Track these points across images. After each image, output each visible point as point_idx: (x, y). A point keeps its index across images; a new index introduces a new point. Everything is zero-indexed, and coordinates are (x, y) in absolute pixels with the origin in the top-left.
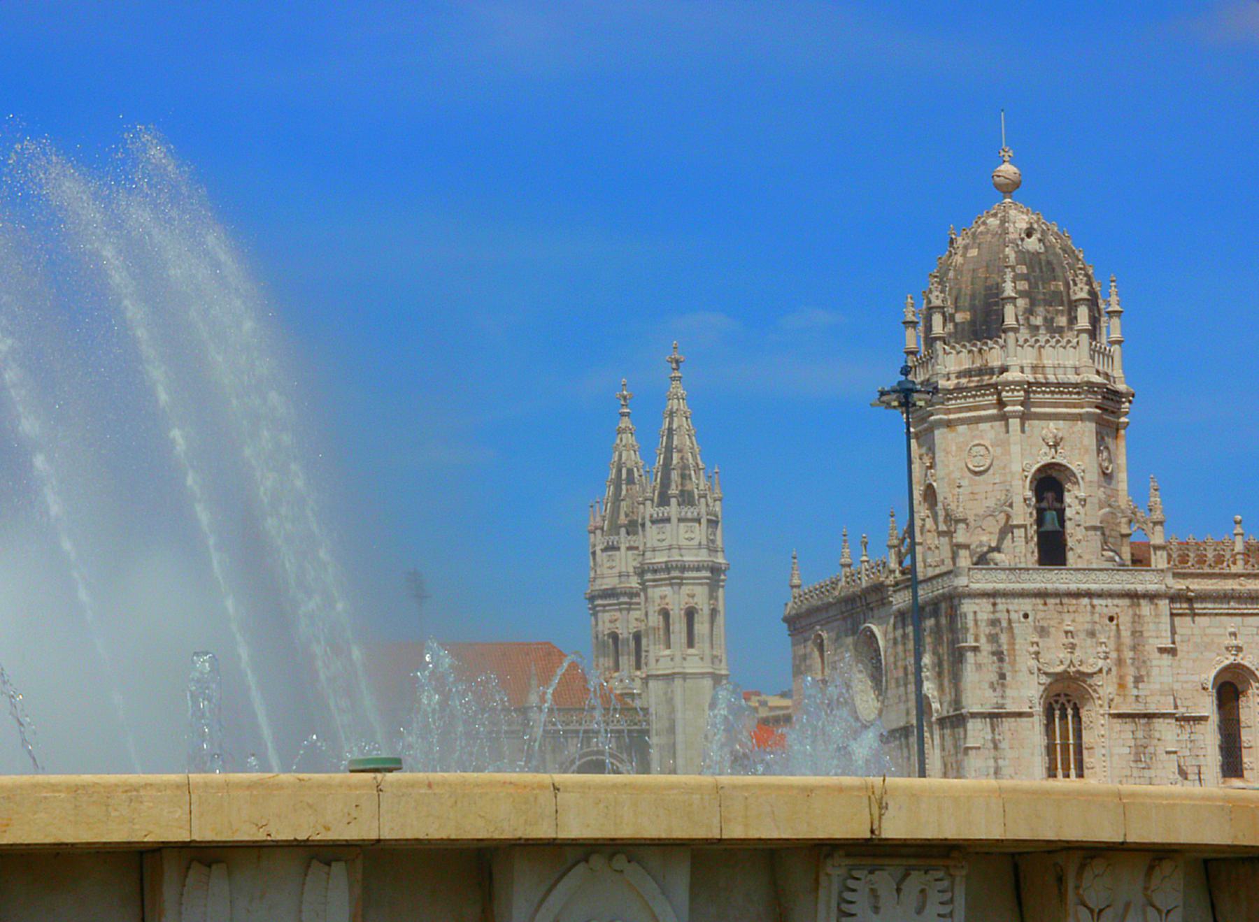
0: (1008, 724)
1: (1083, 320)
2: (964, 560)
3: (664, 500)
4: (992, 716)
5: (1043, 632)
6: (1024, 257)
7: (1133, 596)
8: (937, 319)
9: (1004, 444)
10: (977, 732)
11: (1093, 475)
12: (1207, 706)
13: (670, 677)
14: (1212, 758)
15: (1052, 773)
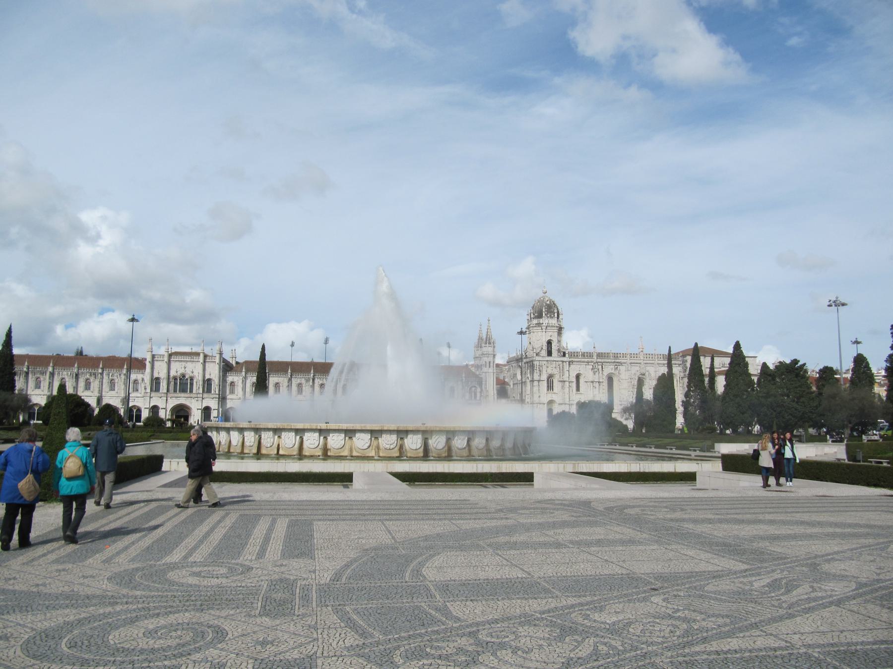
0: (541, 382)
1: (556, 315)
2: (535, 354)
3: (486, 344)
4: (539, 381)
5: (547, 367)
6: (547, 304)
7: (563, 362)
8: (532, 314)
9: (542, 336)
10: (536, 383)
11: (557, 341)
12: (574, 380)
13: (486, 373)
15: (548, 390)
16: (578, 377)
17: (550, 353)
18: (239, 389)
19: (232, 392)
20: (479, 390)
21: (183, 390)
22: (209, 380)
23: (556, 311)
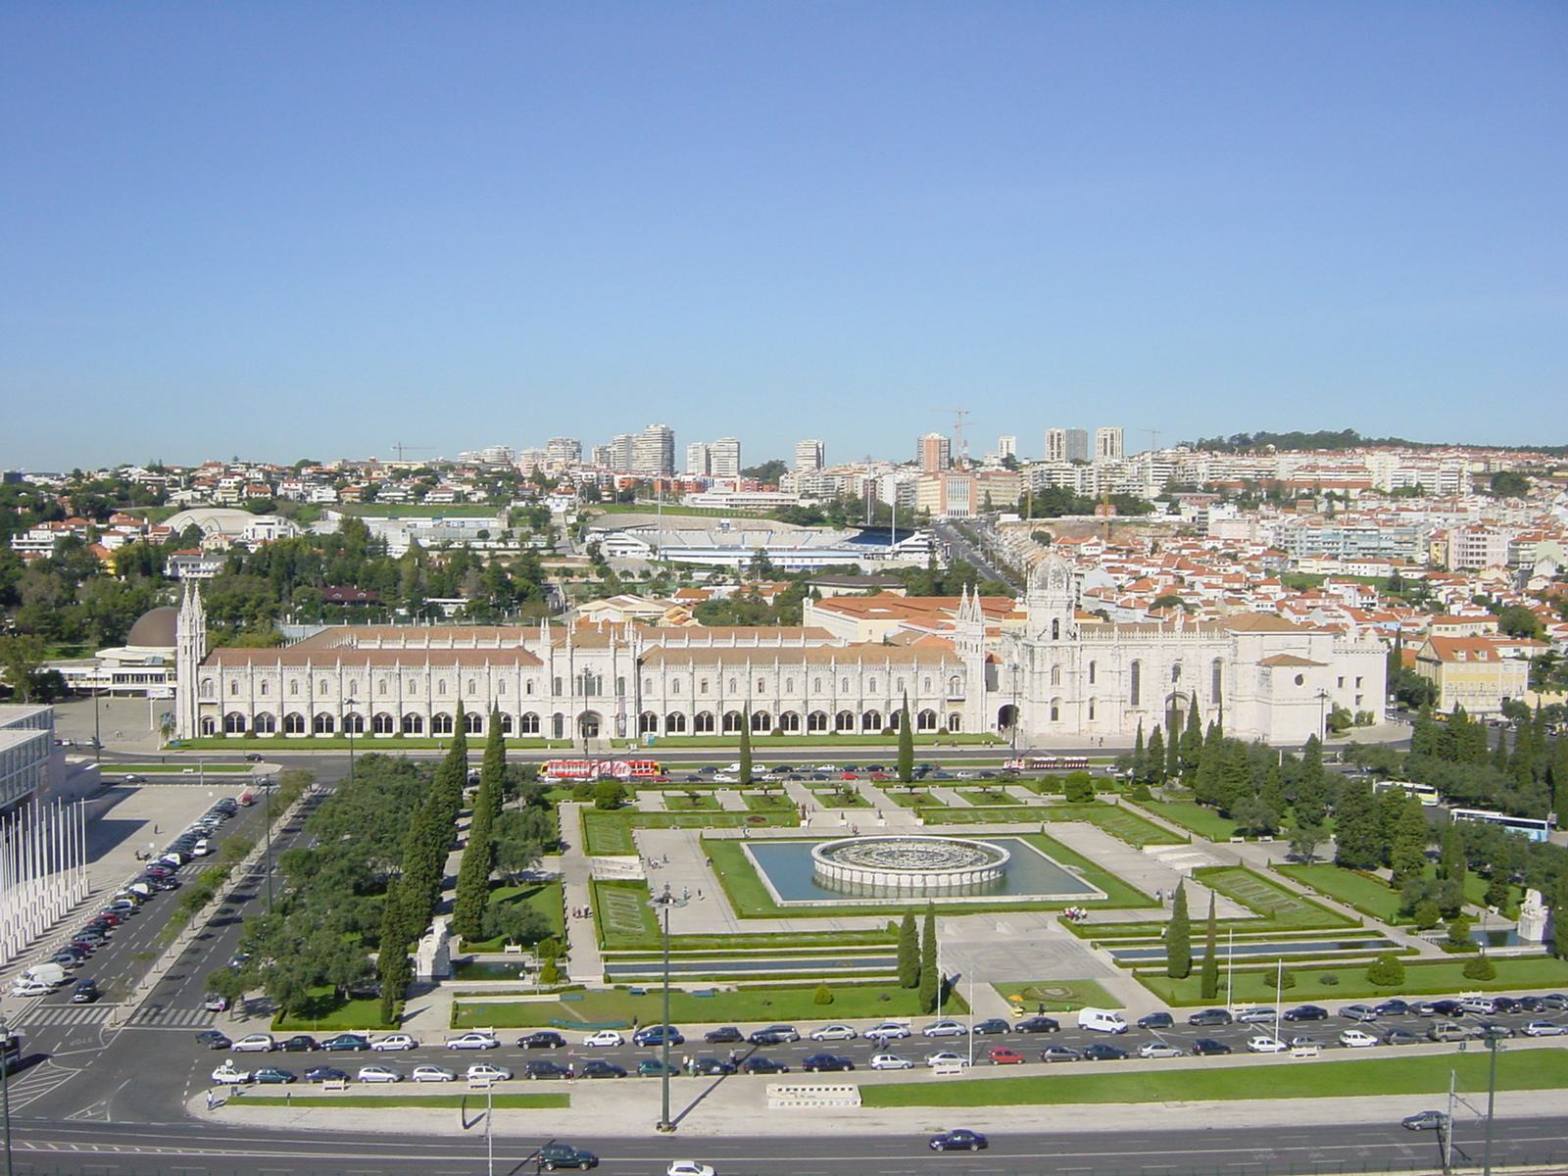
7: (1073, 647)
10: (1036, 676)
12: (1088, 670)
14: (1089, 680)
16: (1092, 665)
17: (1056, 636)
18: (657, 687)
19: (649, 691)
20: (962, 681)
21: (590, 692)
22: (621, 679)
23: (1065, 580)
